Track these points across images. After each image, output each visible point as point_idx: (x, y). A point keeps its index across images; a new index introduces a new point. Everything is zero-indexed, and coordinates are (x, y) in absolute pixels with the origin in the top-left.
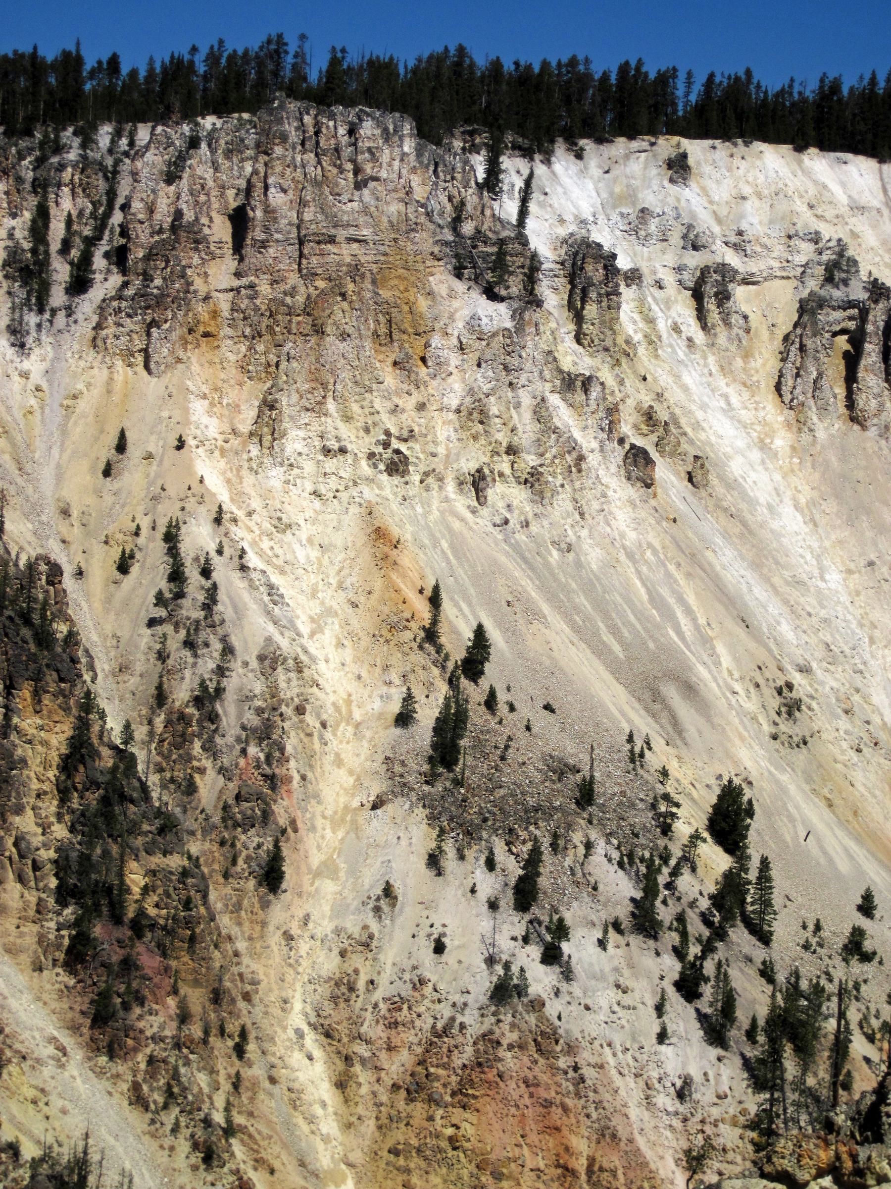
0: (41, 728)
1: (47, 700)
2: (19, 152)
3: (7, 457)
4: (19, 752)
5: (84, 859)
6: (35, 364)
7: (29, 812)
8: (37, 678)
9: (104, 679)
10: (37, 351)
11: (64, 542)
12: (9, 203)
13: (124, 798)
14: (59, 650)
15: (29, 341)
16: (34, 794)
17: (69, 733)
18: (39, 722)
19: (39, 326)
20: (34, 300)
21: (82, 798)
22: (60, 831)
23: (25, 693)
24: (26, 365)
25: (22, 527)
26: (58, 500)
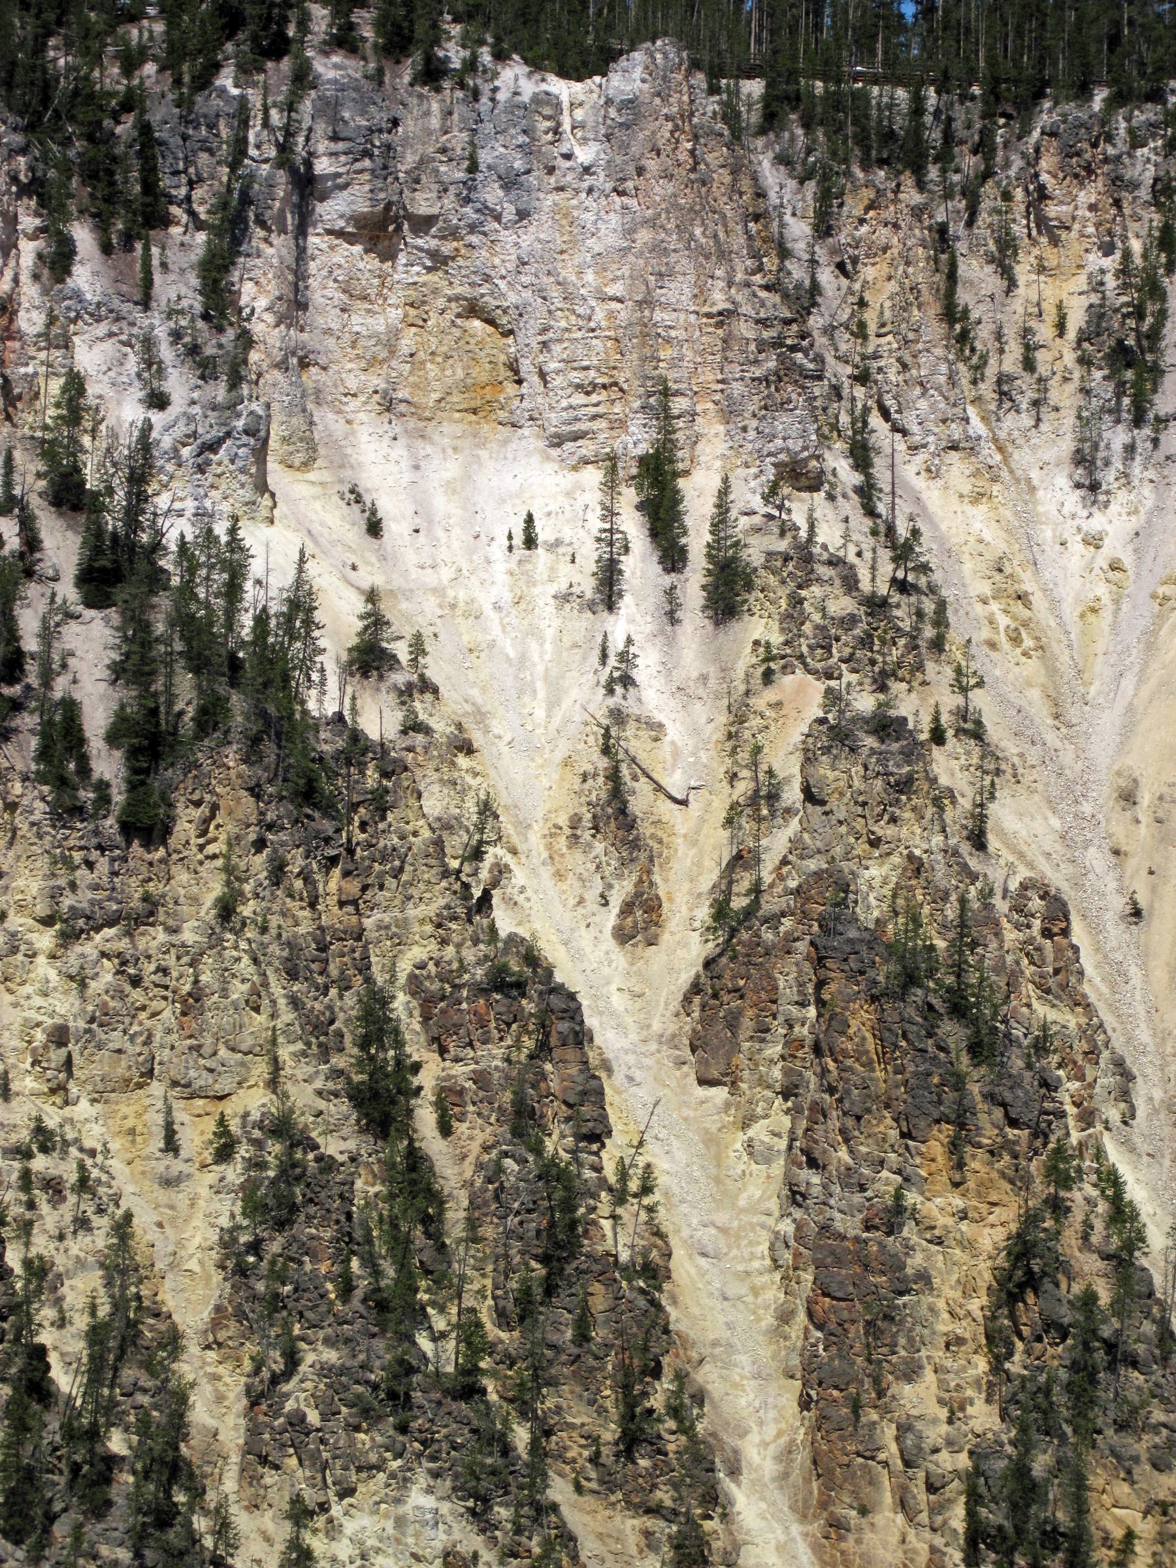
0: (963, 1215)
1: (977, 1163)
2: (1131, 131)
3: (1035, 694)
4: (916, 1261)
5: (1021, 1471)
6: (1115, 522)
7: (929, 1376)
8: (961, 1120)
9: (1149, 1117)
10: (1121, 497)
11: (1116, 852)
12: (1098, 225)
13: (1118, 1355)
14: (1017, 1063)
15: (1108, 477)
16: (942, 1342)
17: (1014, 1227)
18: (958, 1202)
19: (1130, 449)
20: (1126, 401)
21: (1028, 1353)
22: (983, 1417)
23: (936, 1145)
24: (1097, 522)
25: (1038, 826)
26: (1119, 774)
